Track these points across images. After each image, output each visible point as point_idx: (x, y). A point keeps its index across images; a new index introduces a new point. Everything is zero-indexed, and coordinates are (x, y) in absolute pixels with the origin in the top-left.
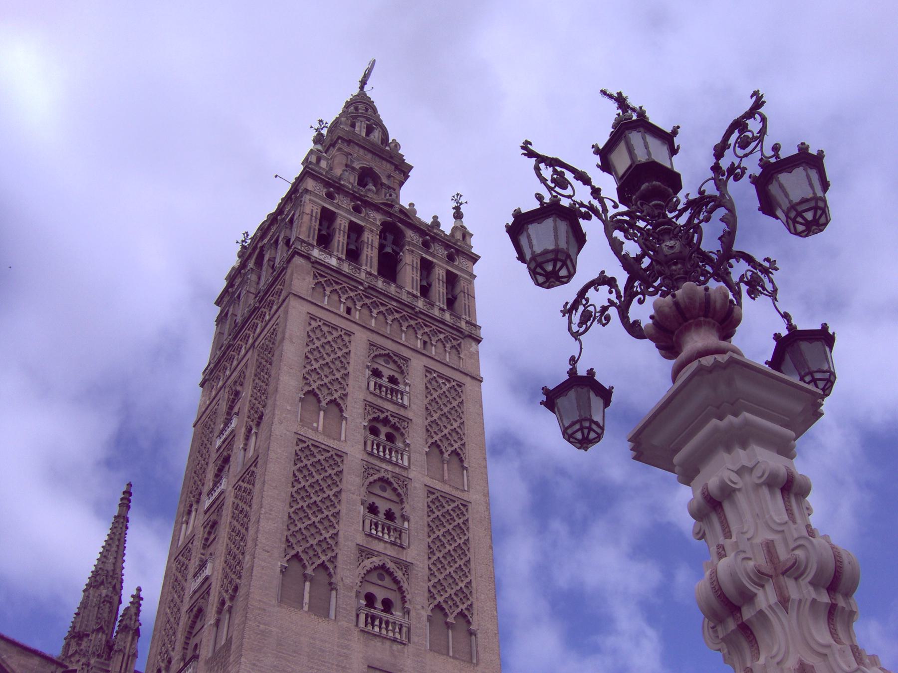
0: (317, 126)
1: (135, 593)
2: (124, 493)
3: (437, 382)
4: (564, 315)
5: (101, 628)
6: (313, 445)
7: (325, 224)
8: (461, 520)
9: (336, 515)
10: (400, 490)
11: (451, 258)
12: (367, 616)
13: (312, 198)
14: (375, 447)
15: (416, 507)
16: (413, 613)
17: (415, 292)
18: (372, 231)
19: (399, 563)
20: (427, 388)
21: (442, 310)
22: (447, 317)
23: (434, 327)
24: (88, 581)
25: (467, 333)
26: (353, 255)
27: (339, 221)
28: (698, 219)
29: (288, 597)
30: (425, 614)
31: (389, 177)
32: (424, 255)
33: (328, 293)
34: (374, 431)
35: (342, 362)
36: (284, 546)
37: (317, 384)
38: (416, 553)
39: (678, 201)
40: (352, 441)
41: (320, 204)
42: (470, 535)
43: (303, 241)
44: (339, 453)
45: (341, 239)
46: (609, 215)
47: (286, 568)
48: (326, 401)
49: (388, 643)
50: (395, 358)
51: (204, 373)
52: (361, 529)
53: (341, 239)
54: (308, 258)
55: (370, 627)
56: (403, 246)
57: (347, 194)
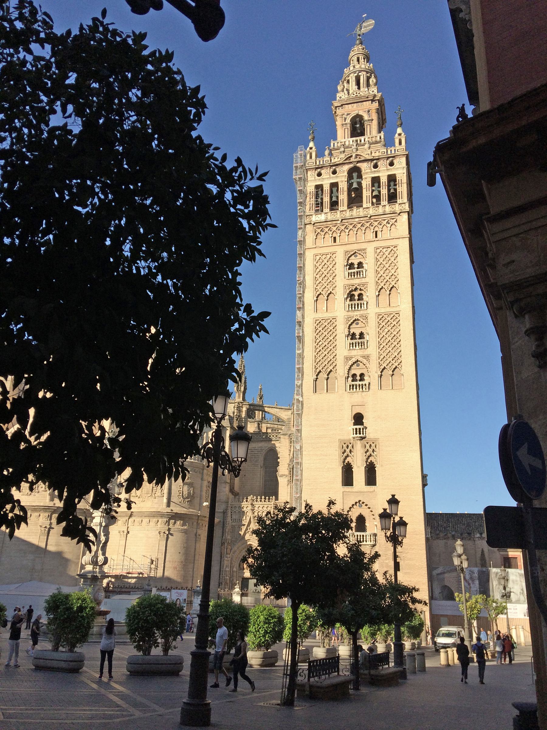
10: (364, 321)
12: (350, 386)
17: (368, 206)
19: (363, 357)
22: (388, 209)
23: (380, 220)
26: (334, 205)
32: (373, 175)
38: (372, 349)
40: (339, 309)
42: (401, 328)
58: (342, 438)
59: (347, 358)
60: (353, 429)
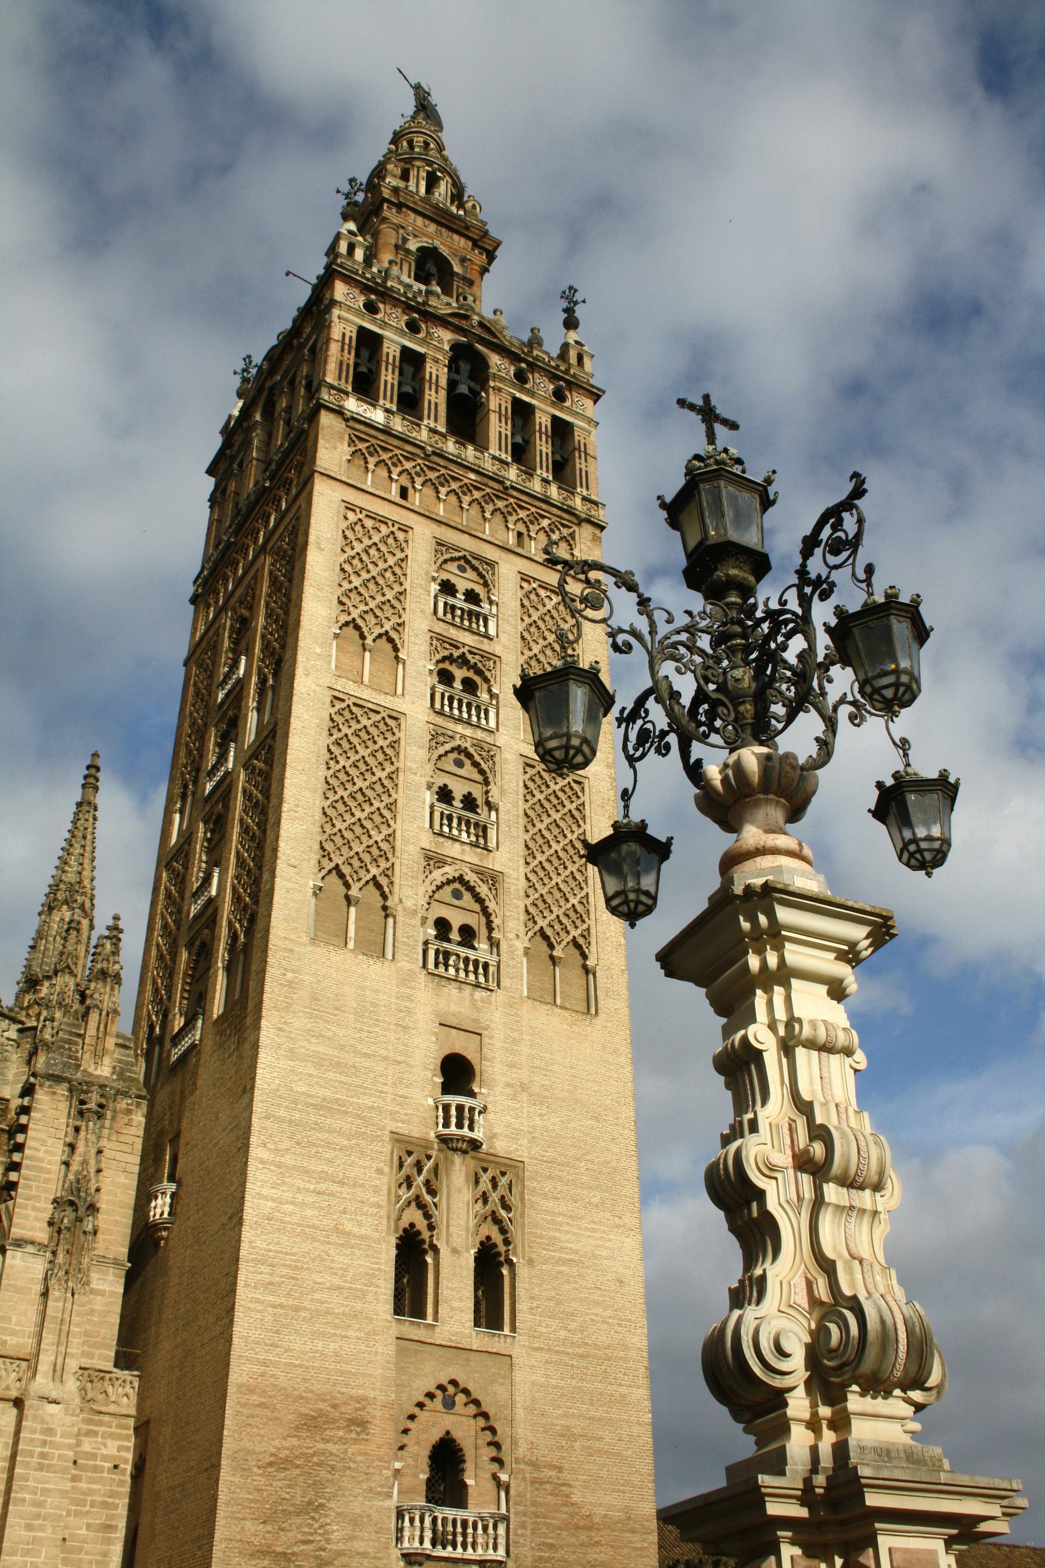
0: (346, 188)
1: (111, 923)
2: (88, 767)
3: (537, 595)
4: (619, 727)
6: (355, 704)
7: (365, 353)
8: (574, 805)
9: (391, 807)
10: (484, 766)
11: (559, 396)
12: (437, 952)
13: (344, 314)
14: (446, 702)
16: (503, 946)
17: (503, 456)
18: (436, 361)
19: (480, 872)
20: (523, 606)
21: (545, 481)
22: (554, 491)
23: (533, 510)
24: (43, 899)
25: (584, 516)
26: (410, 403)
27: (386, 344)
28: (775, 641)
29: (329, 931)
30: (520, 945)
31: (463, 260)
32: (518, 395)
33: (371, 466)
34: (445, 677)
35: (394, 574)
36: (318, 857)
37: (358, 611)
38: (508, 856)
39: (755, 606)
41: (354, 324)
43: (332, 387)
44: (394, 714)
45: (389, 378)
46: (658, 637)
47: (320, 889)
48: (374, 636)
49: (468, 989)
50: (474, 562)
51: (195, 582)
52: (427, 825)
53: (389, 378)
54: (339, 412)
56: (487, 380)
57: (396, 302)
58: (403, 1128)
59: (428, 858)
60: (446, 1108)
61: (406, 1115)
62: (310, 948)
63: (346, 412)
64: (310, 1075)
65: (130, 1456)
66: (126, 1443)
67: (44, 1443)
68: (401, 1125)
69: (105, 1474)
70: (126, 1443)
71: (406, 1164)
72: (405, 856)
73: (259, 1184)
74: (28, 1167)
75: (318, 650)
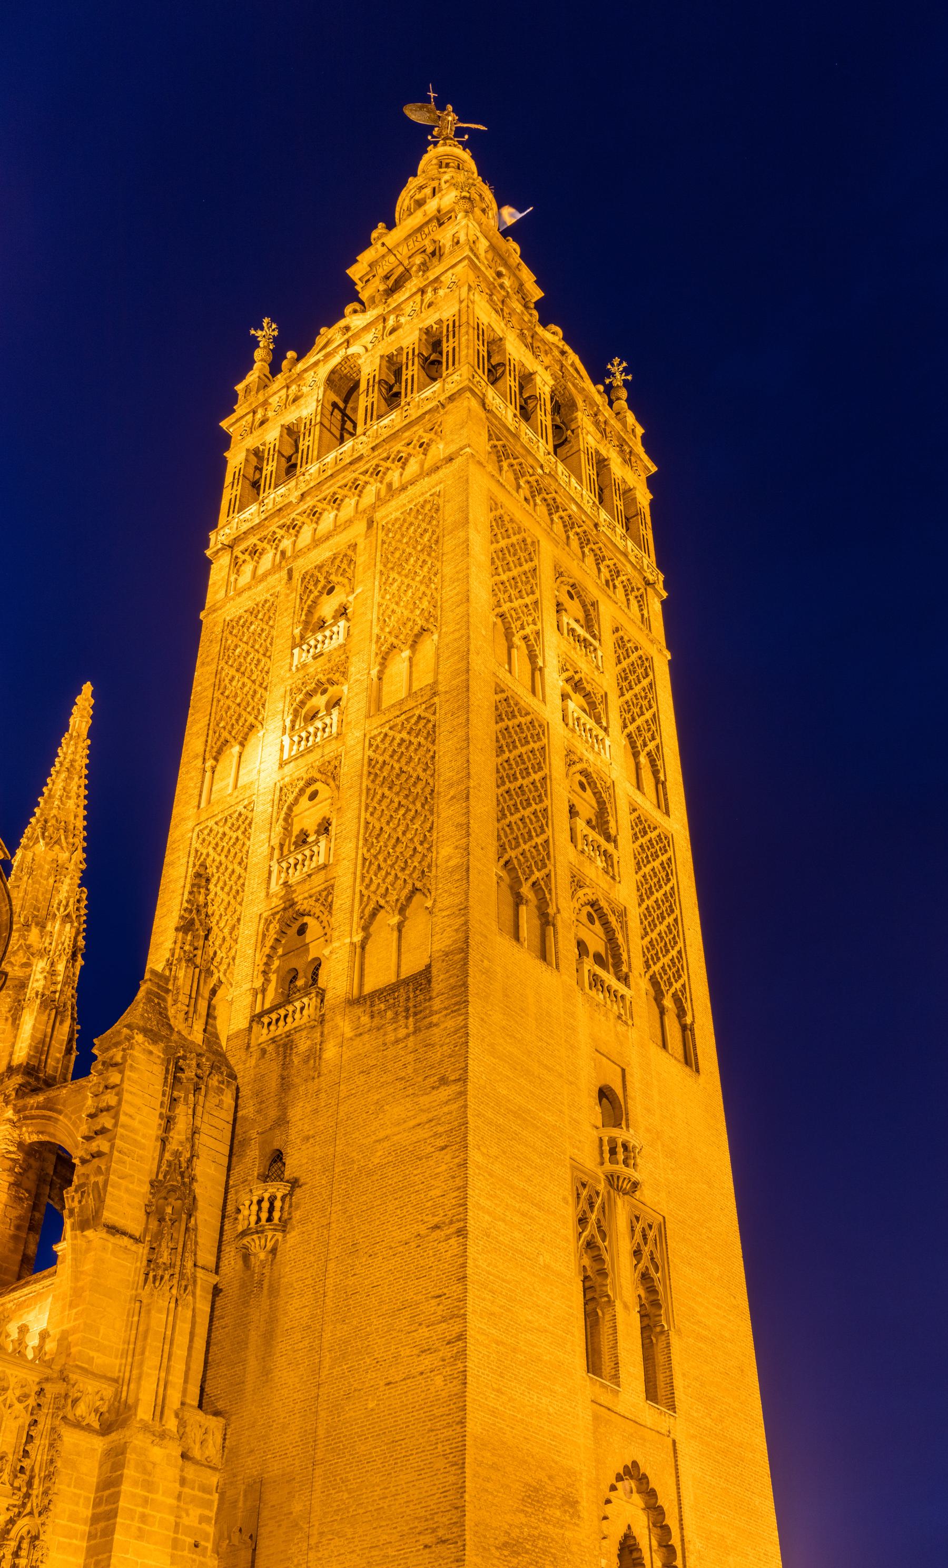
5: (68, 916)
10: (603, 795)
15: (622, 823)
23: (615, 560)
33: (505, 464)
38: (625, 893)
45: (512, 383)
55: (593, 993)
61: (580, 1142)
62: (499, 939)
63: (487, 401)
64: (508, 1077)
65: (210, 1529)
66: (207, 1512)
67: (146, 1501)
68: (576, 1151)
69: (186, 1553)
70: (207, 1512)
71: (582, 1197)
72: (558, 865)
73: (477, 1191)
74: (122, 1137)
75: (484, 632)
